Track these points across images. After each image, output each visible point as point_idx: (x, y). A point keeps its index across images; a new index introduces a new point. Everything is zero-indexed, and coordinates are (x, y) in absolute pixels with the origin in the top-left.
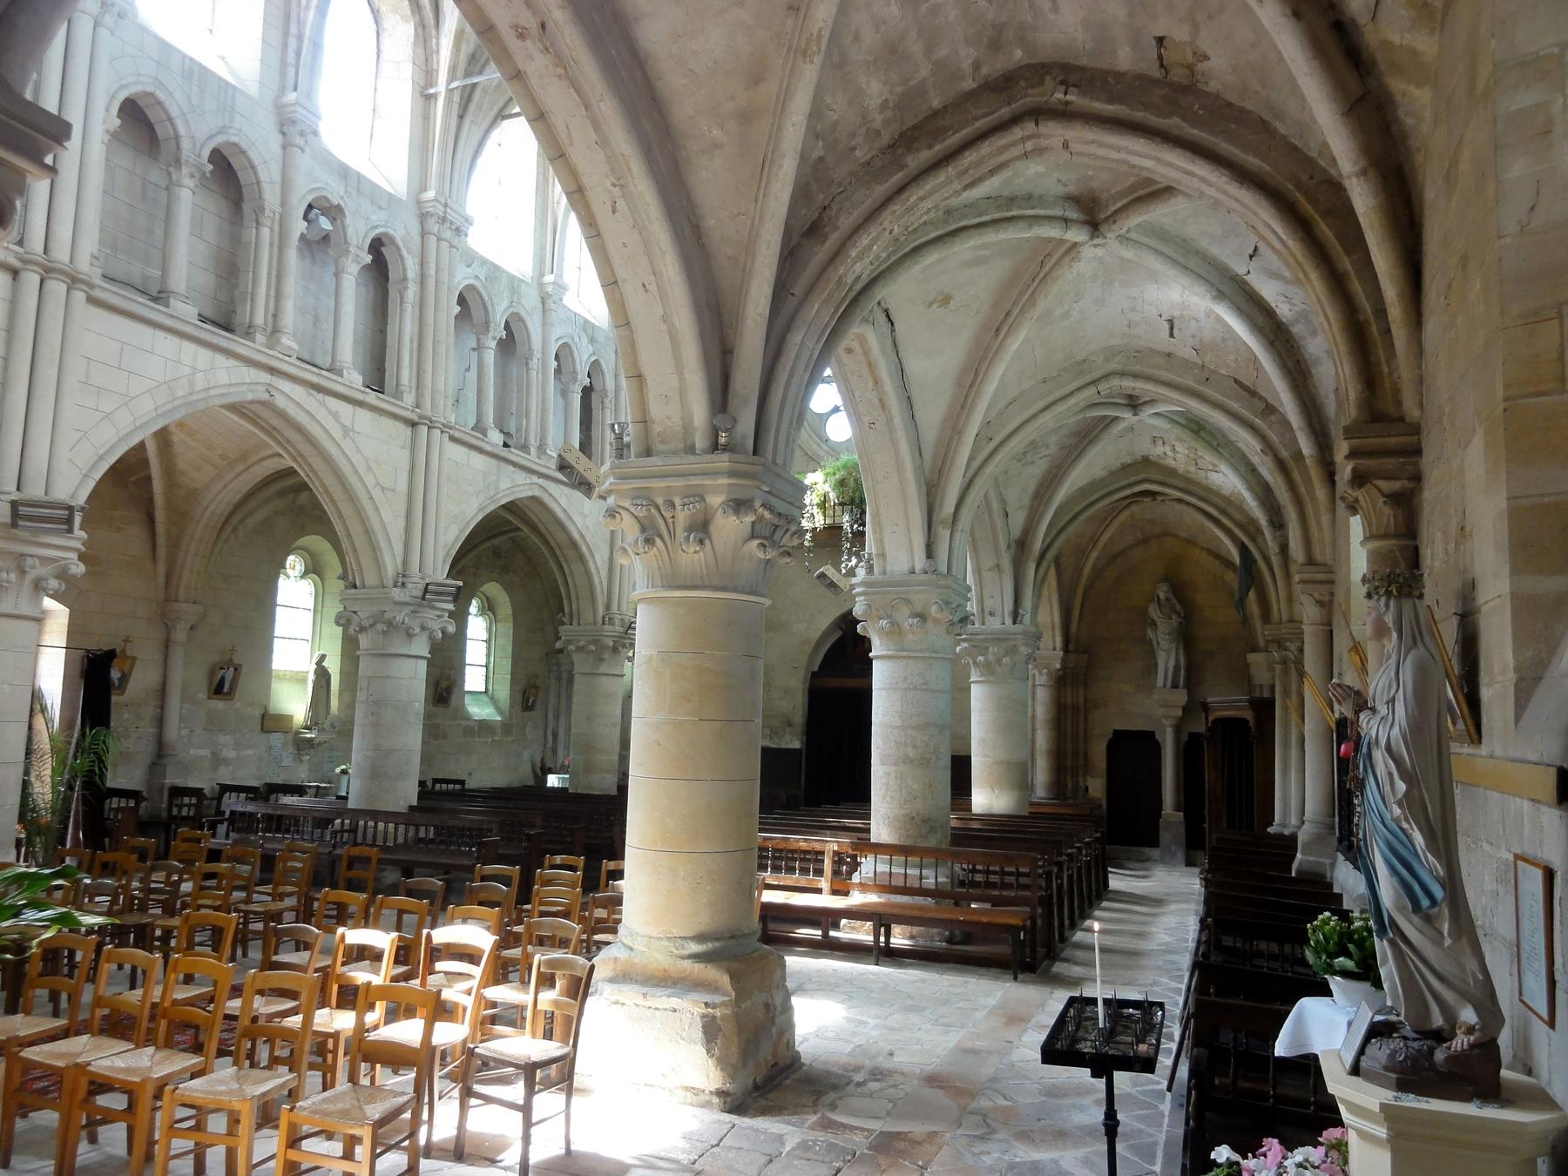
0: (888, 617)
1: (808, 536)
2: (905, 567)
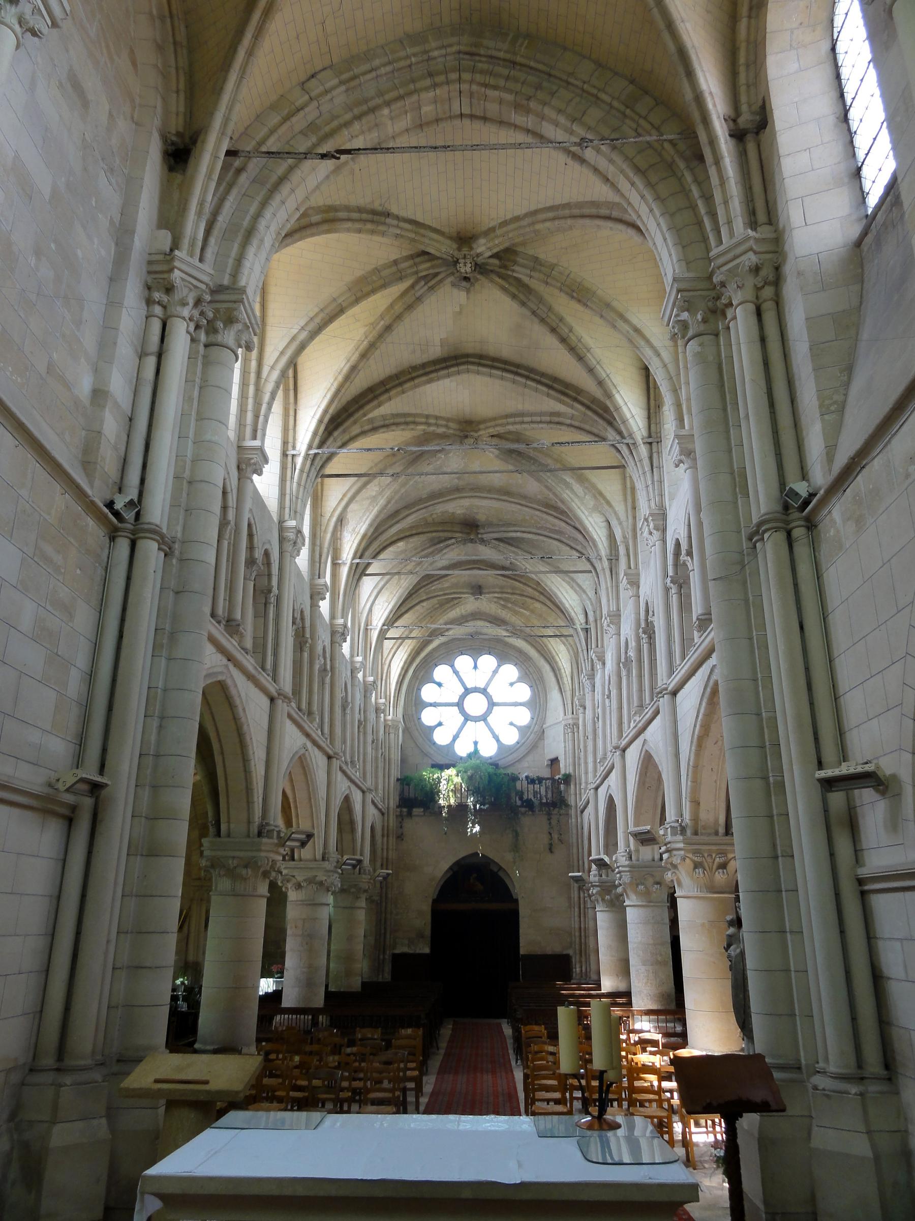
0: (642, 884)
1: (446, 810)
2: (650, 858)
